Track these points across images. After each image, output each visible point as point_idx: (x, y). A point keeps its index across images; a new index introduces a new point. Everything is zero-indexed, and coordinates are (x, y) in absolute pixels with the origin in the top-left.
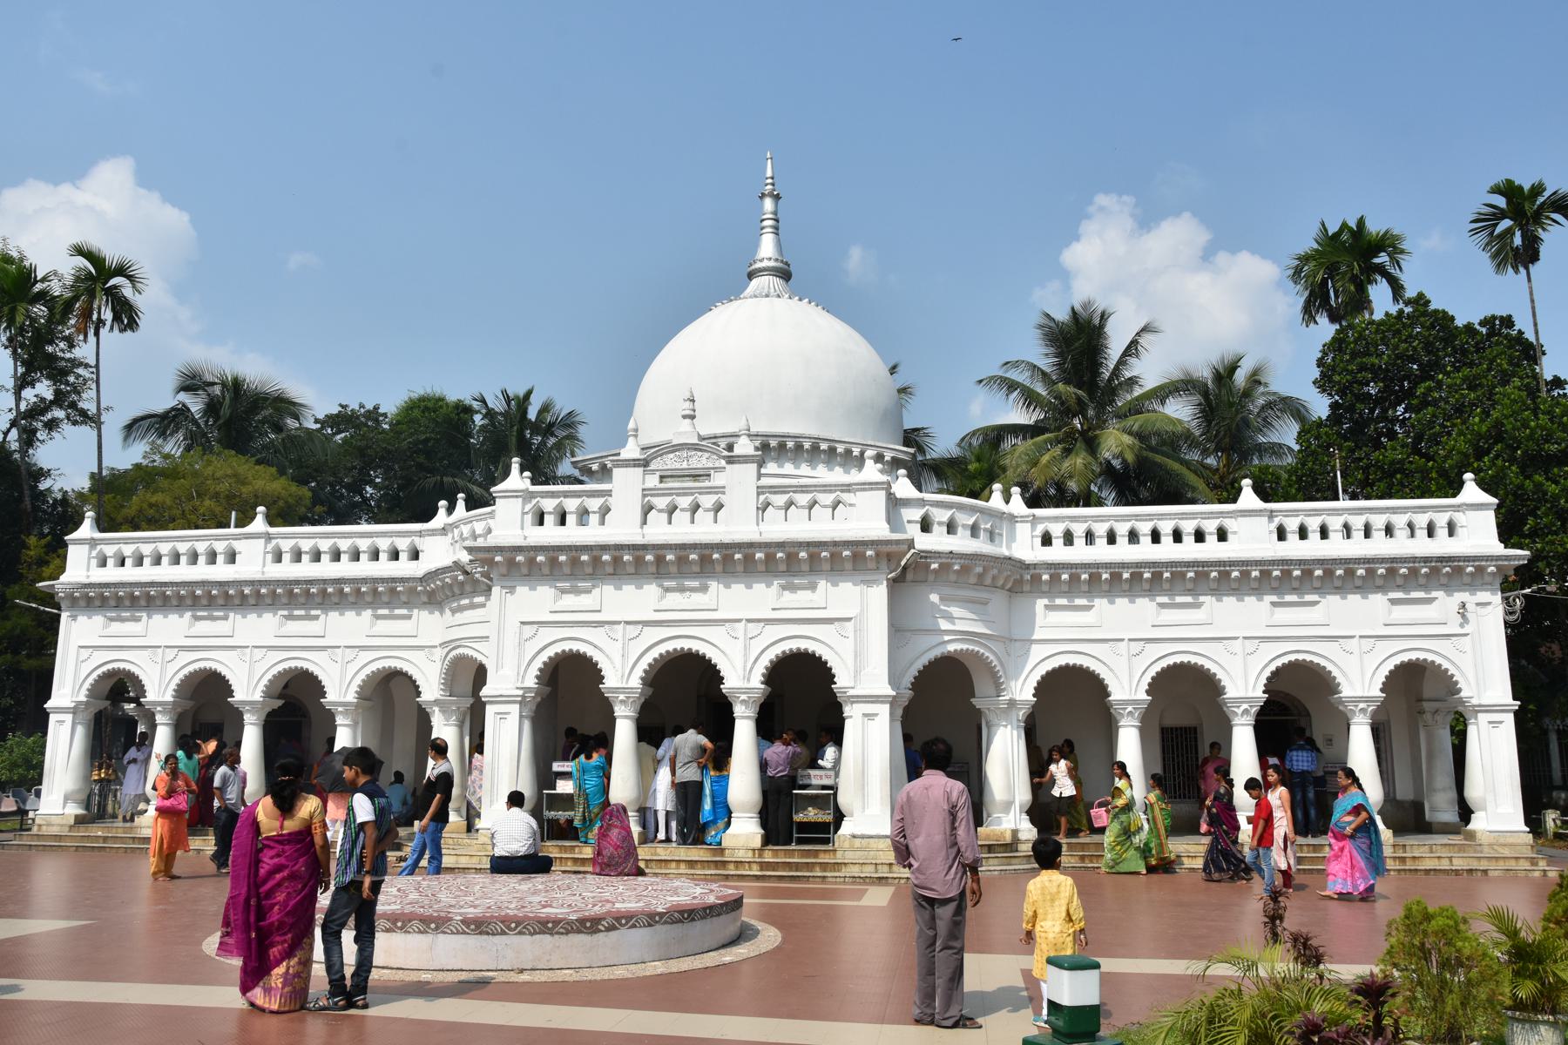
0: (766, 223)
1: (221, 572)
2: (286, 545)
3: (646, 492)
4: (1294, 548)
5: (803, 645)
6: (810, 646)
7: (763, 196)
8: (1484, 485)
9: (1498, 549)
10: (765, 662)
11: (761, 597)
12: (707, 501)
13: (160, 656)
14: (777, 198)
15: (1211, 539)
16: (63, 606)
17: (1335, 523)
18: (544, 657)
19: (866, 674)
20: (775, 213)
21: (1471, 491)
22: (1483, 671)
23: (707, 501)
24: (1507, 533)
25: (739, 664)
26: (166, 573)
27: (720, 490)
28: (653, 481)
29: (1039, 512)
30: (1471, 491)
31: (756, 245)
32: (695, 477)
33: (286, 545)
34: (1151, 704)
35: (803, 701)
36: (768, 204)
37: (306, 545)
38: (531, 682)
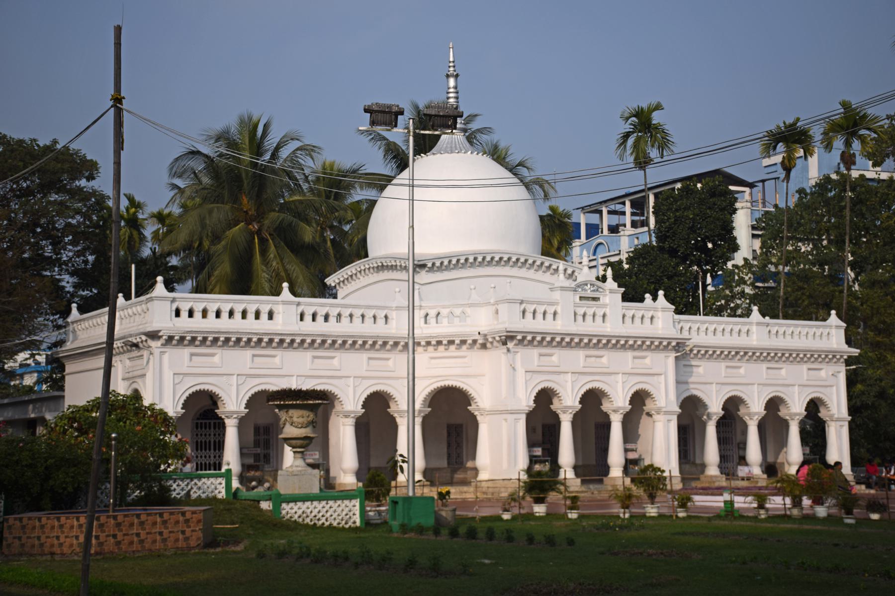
0: (451, 95)
1: (264, 326)
3: (576, 305)
7: (448, 76)
8: (839, 315)
9: (845, 347)
14: (457, 76)
15: (743, 335)
19: (666, 400)
20: (455, 87)
21: (834, 318)
24: (849, 342)
26: (224, 324)
27: (605, 306)
30: (834, 318)
32: (594, 299)
34: (766, 415)
38: (532, 403)
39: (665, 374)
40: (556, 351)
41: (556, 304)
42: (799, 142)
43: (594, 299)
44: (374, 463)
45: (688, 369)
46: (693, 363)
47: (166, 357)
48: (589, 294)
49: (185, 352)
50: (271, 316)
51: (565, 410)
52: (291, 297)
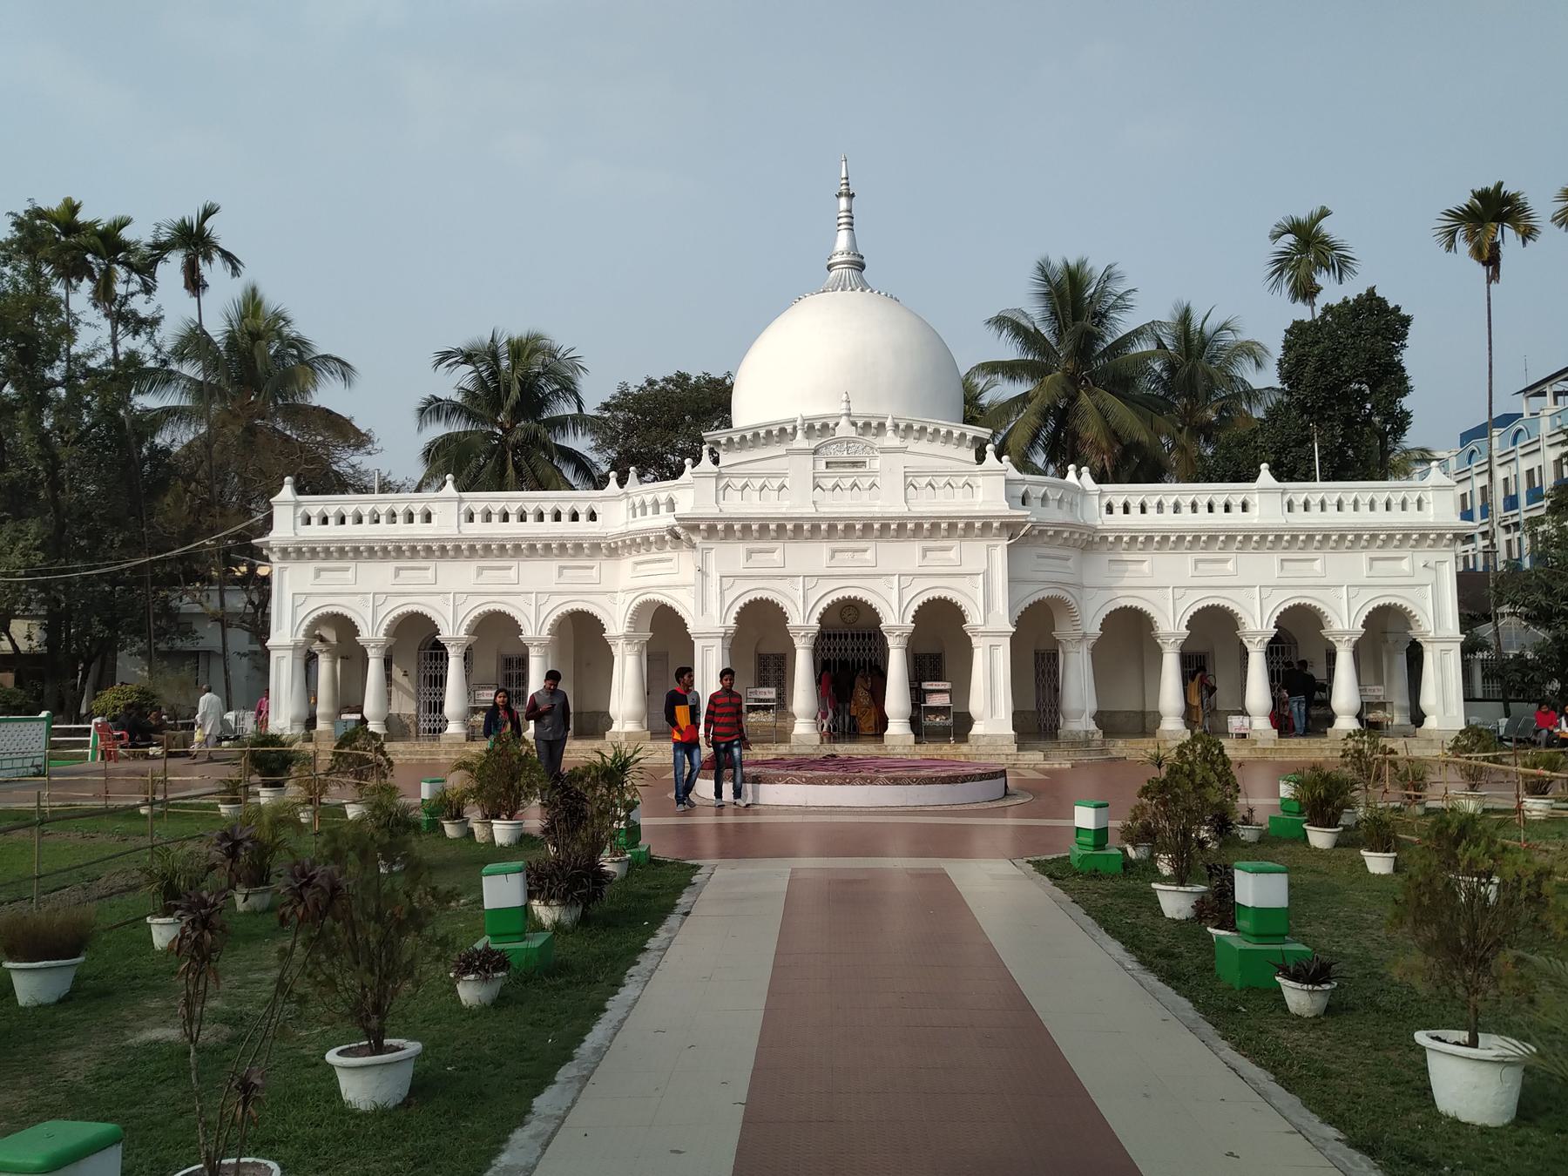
2: (478, 508)
4: (1299, 519)
5: (943, 594)
6: (949, 595)
10: (914, 607)
11: (908, 554)
12: (866, 482)
13: (373, 600)
14: (851, 196)
16: (273, 558)
17: (1315, 500)
18: (741, 603)
22: (1437, 616)
23: (866, 482)
25: (895, 606)
26: (367, 531)
27: (874, 473)
28: (822, 466)
29: (1105, 487)
31: (835, 240)
32: (854, 464)
33: (478, 508)
35: (940, 639)
36: (843, 202)
37: (496, 508)
38: (731, 622)
39: (987, 576)
40: (778, 545)
41: (785, 475)
42: (1501, 218)
43: (854, 464)
44: (394, 710)
45: (1114, 567)
46: (1126, 557)
47: (287, 574)
48: (844, 456)
49: (309, 567)
50: (428, 518)
51: (891, 629)
52: (456, 494)
